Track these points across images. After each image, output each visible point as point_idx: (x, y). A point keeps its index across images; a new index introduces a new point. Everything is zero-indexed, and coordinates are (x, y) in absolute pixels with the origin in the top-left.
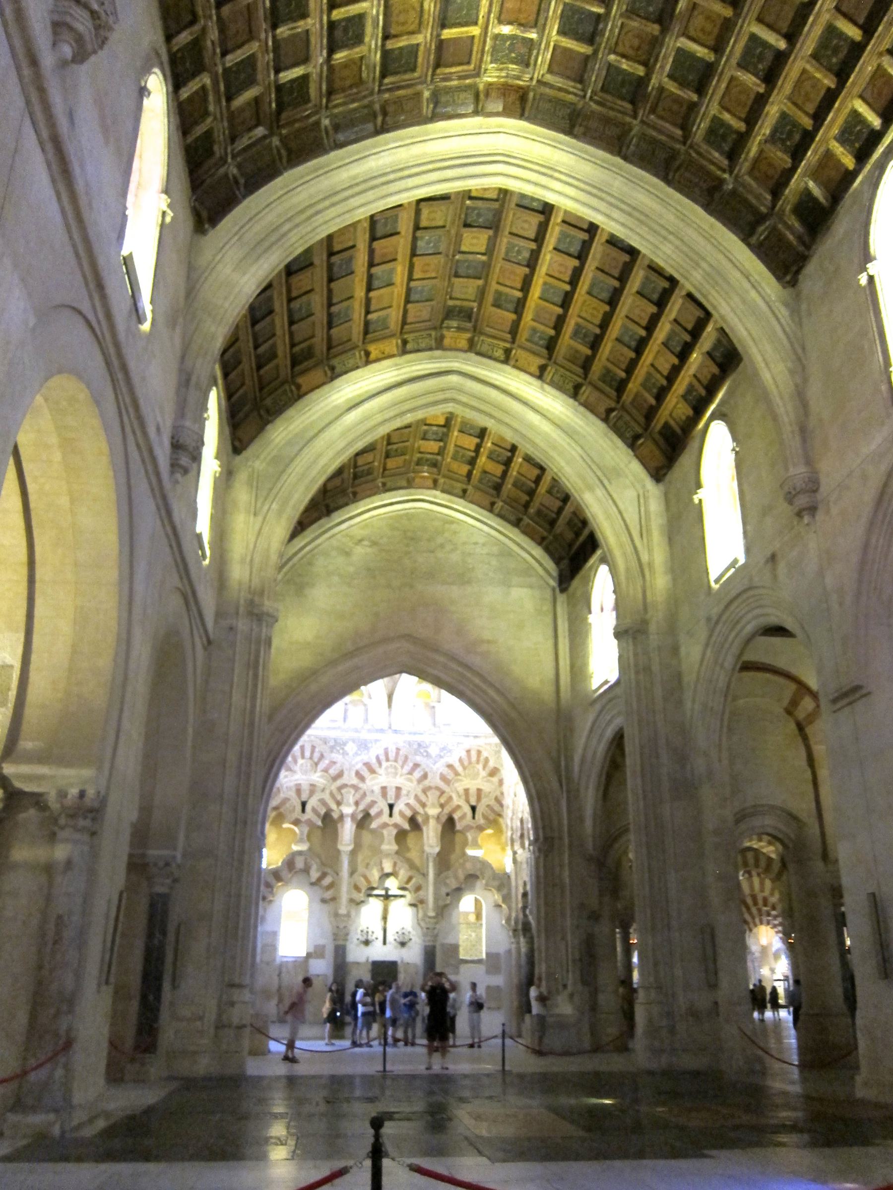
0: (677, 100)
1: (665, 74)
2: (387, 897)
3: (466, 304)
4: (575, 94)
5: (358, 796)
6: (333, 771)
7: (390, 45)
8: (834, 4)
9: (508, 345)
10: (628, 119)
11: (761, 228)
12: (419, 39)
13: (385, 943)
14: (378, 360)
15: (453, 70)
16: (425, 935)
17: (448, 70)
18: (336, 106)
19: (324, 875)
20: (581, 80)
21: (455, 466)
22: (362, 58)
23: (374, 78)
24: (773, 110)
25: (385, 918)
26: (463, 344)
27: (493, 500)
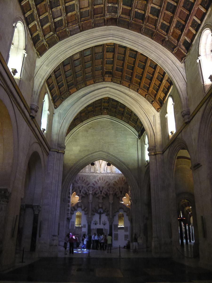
0: (152, 19)
2: (100, 214)
3: (109, 70)
4: (129, 19)
5: (93, 189)
6: (87, 183)
9: (121, 80)
10: (142, 24)
13: (100, 224)
15: (98, 15)
16: (109, 222)
18: (70, 26)
22: (75, 14)
24: (175, 20)
25: (100, 218)
26: (110, 80)
27: (122, 117)
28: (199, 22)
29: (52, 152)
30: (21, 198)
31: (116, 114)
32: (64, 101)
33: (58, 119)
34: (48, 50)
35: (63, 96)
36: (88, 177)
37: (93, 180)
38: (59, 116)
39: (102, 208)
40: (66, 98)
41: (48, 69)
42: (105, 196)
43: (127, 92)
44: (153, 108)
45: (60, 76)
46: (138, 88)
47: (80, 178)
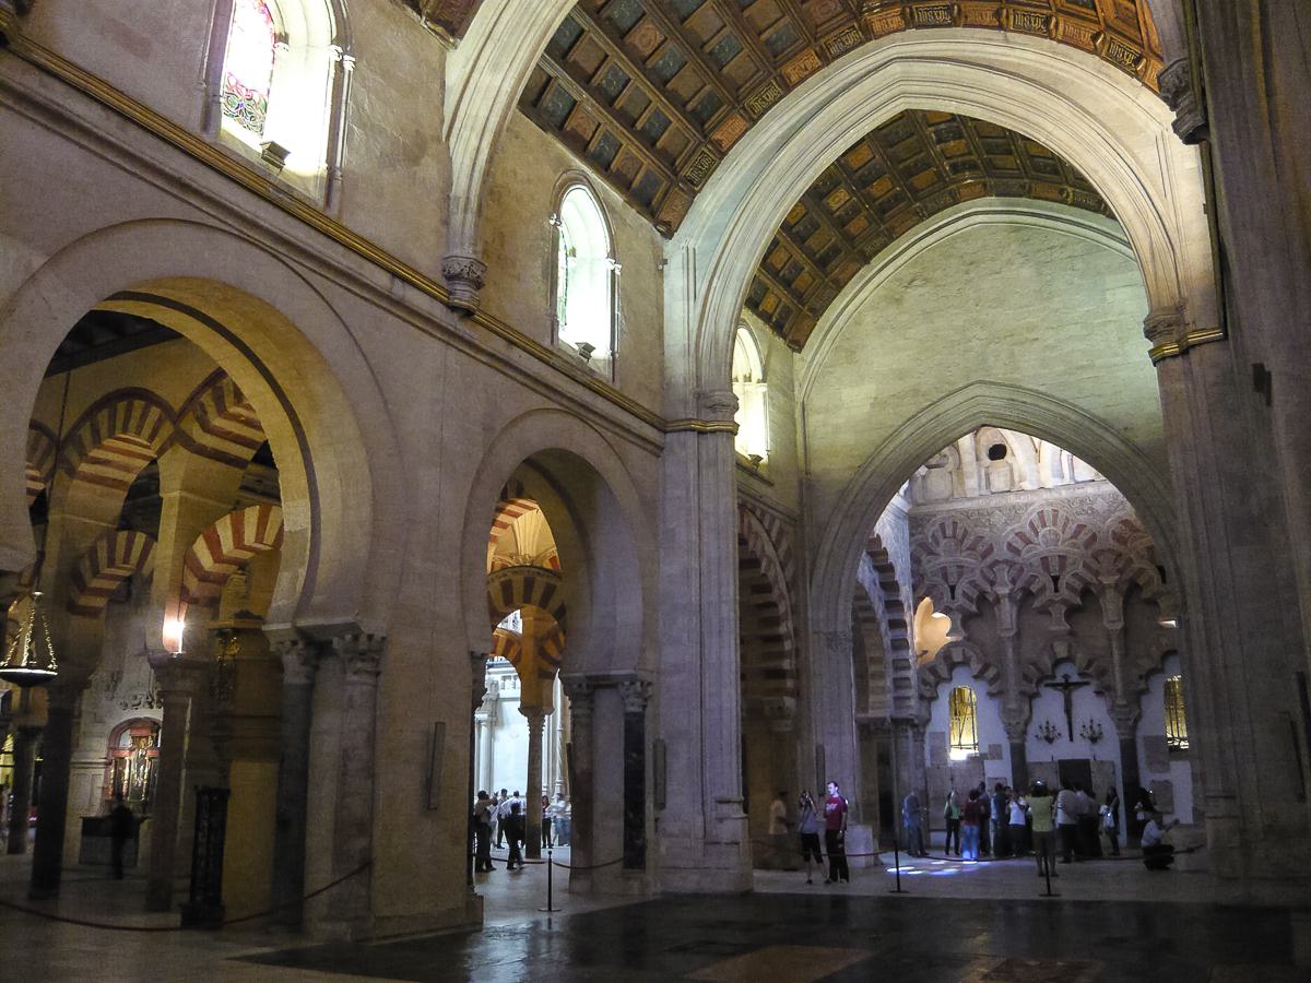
2: (1067, 687)
6: (981, 548)
13: (1071, 740)
14: (802, 80)
19: (986, 667)
26: (897, 21)
29: (675, 435)
30: (472, 654)
31: (1026, 180)
32: (699, 191)
36: (980, 516)
37: (1009, 528)
38: (691, 266)
39: (1069, 659)
40: (706, 175)
41: (497, 84)
42: (1078, 601)
46: (1045, 12)
47: (942, 526)
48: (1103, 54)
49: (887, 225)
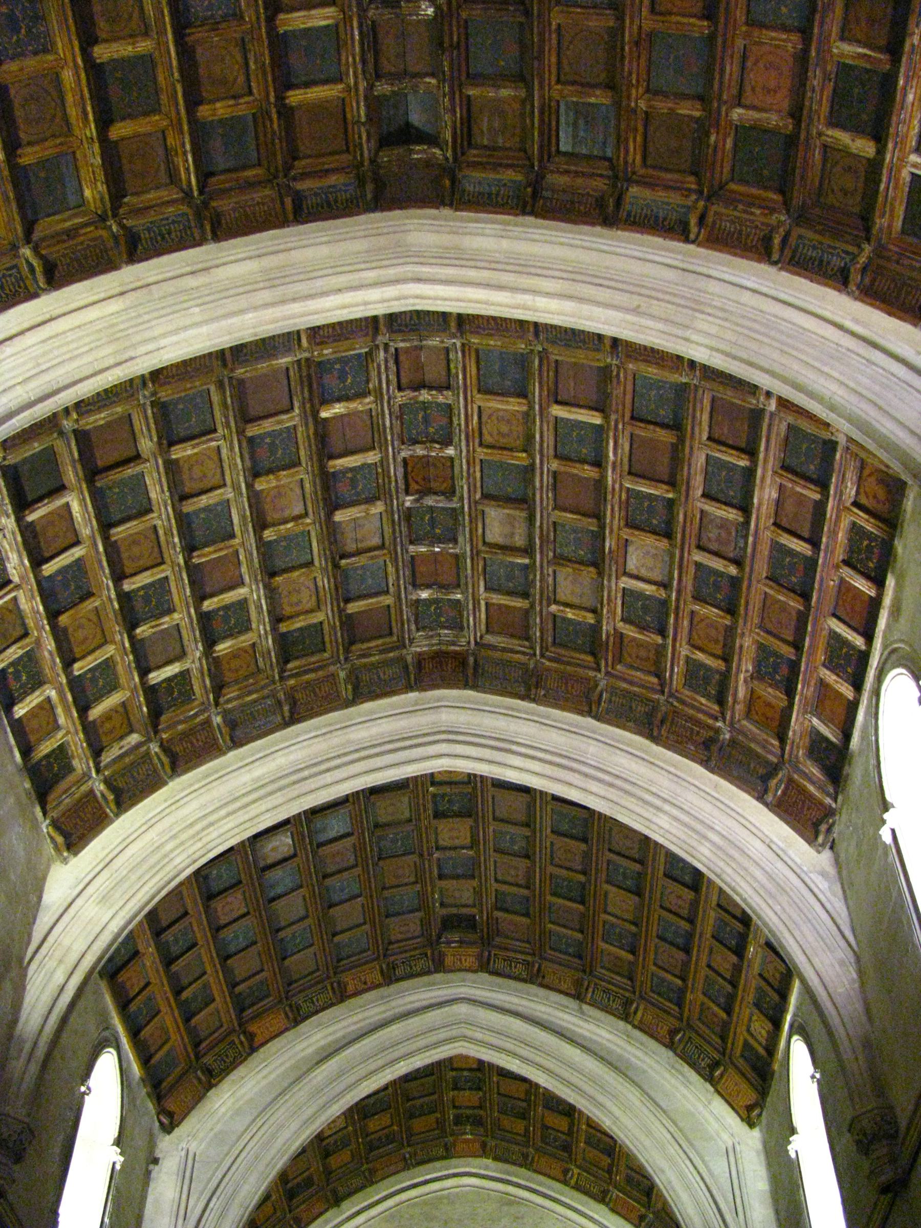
0: (640, 645)
1: (618, 618)
3: (464, 911)
4: (524, 653)
7: (283, 628)
8: (772, 521)
9: (529, 958)
10: (591, 674)
11: (773, 783)
12: (320, 617)
15: (373, 644)
17: (365, 646)
18: (229, 701)
20: (528, 639)
21: (506, 1122)
22: (254, 645)
23: (271, 665)
26: (470, 961)
28: (859, 642)
32: (216, 1085)
33: (177, 1195)
34: (112, 822)
35: (208, 1060)
38: (187, 1176)
43: (569, 1022)
44: (719, 1107)
45: (189, 949)
46: (627, 994)
48: (678, 1051)
49: (370, 1165)
